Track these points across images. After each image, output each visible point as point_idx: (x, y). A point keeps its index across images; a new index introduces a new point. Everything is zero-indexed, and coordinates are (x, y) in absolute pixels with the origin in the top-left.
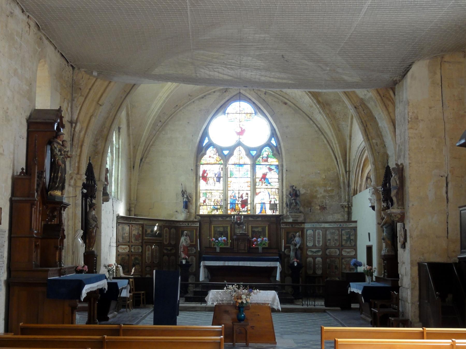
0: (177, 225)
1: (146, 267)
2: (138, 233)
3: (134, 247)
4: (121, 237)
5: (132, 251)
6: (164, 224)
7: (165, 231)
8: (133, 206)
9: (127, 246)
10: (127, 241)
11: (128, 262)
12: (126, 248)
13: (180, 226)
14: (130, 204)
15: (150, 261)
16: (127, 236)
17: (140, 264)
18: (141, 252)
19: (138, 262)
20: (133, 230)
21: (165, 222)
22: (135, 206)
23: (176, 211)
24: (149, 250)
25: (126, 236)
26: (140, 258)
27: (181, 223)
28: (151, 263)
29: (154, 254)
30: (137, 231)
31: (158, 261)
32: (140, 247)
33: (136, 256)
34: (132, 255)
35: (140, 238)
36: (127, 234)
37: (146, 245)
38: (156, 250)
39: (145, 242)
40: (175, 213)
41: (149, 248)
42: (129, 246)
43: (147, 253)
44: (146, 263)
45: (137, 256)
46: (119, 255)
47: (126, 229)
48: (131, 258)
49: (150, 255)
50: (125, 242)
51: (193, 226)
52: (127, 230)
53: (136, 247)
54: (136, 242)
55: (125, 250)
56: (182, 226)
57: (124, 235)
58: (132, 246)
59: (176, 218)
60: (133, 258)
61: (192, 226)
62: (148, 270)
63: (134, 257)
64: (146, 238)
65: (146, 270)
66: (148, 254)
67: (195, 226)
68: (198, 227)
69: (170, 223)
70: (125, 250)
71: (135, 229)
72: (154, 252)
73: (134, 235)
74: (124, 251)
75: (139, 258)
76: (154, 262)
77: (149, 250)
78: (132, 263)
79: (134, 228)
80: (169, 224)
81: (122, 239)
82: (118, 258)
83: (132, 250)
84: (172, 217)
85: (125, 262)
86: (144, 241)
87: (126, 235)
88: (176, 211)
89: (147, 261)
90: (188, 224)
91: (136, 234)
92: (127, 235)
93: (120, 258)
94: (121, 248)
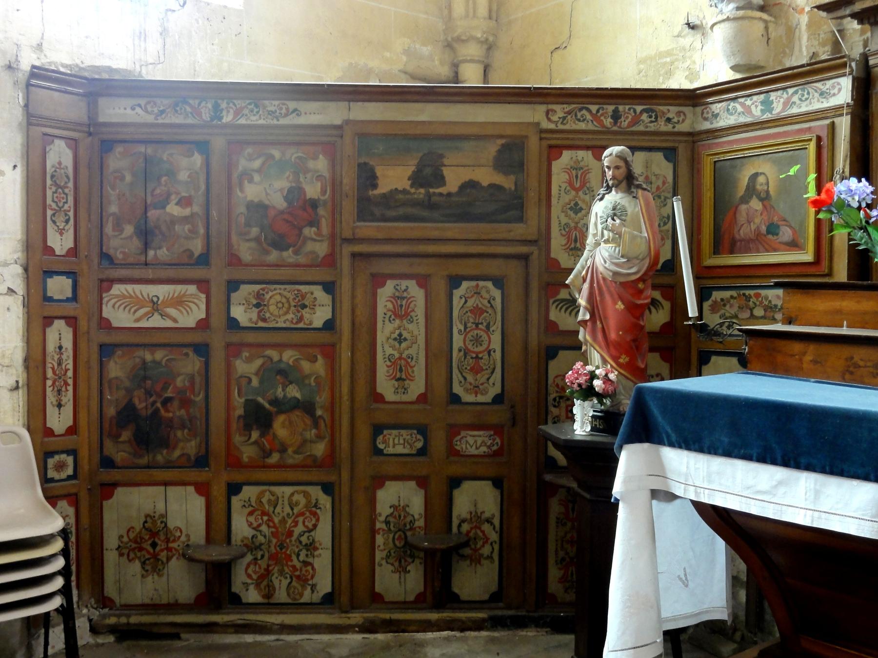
0: (684, 127)
1: (378, 430)
2: (295, 194)
3: (259, 295)
4: (129, 230)
5: (233, 324)
6: (546, 125)
7: (559, 179)
8: (473, 50)
9: (192, 289)
10: (190, 253)
11: (200, 398)
12: (179, 302)
13: (707, 126)
14: (449, 46)
15: (417, 387)
16: (185, 220)
17: (319, 412)
18: (329, 325)
19: (294, 392)
20: (247, 176)
21: (559, 110)
22: (490, 47)
23: (692, 27)
24: (402, 312)
25: (173, 221)
26: (320, 366)
27: (717, 108)
28: (423, 398)
29: (458, 341)
30: (282, 184)
31: (497, 390)
32: (318, 292)
33: (274, 354)
34: (233, 350)
35: (308, 231)
36: (184, 202)
37: (378, 280)
38: (477, 311)
39: (354, 255)
40: (691, 39)
41: (397, 298)
42: (203, 285)
43: (385, 330)
44: (379, 398)
45: (289, 356)
46: (106, 350)
47: (171, 174)
48: (229, 367)
49: (418, 351)
50: (163, 254)
51: (804, 108)
52: (183, 176)
53: (275, 295)
54: (274, 256)
55: (172, 311)
56: (722, 123)
57: (152, 214)
58: (233, 286)
59: (692, 75)
60: (246, 367)
61: (795, 110)
62: (400, 450)
63: (259, 362)
64: (368, 229)
65: (379, 452)
66: (400, 339)
67: (817, 105)
68: (837, 110)
69: (616, 116)
70: (172, 311)
71: (259, 171)
72: (457, 326)
73: (258, 208)
74: (156, 321)
75: (306, 366)
76: (455, 399)
77: (402, 312)
78: (238, 401)
79: (257, 164)
80: (608, 122)
81: (136, 244)
82: (102, 365)
83: (238, 312)
84: (669, 74)
85: (169, 394)
86: (347, 249)
87: (173, 209)
88: (692, 27)
89: (386, 387)
90: (767, 105)
91: (279, 202)
92: (187, 212)
93: (116, 369)
94: (136, 302)
